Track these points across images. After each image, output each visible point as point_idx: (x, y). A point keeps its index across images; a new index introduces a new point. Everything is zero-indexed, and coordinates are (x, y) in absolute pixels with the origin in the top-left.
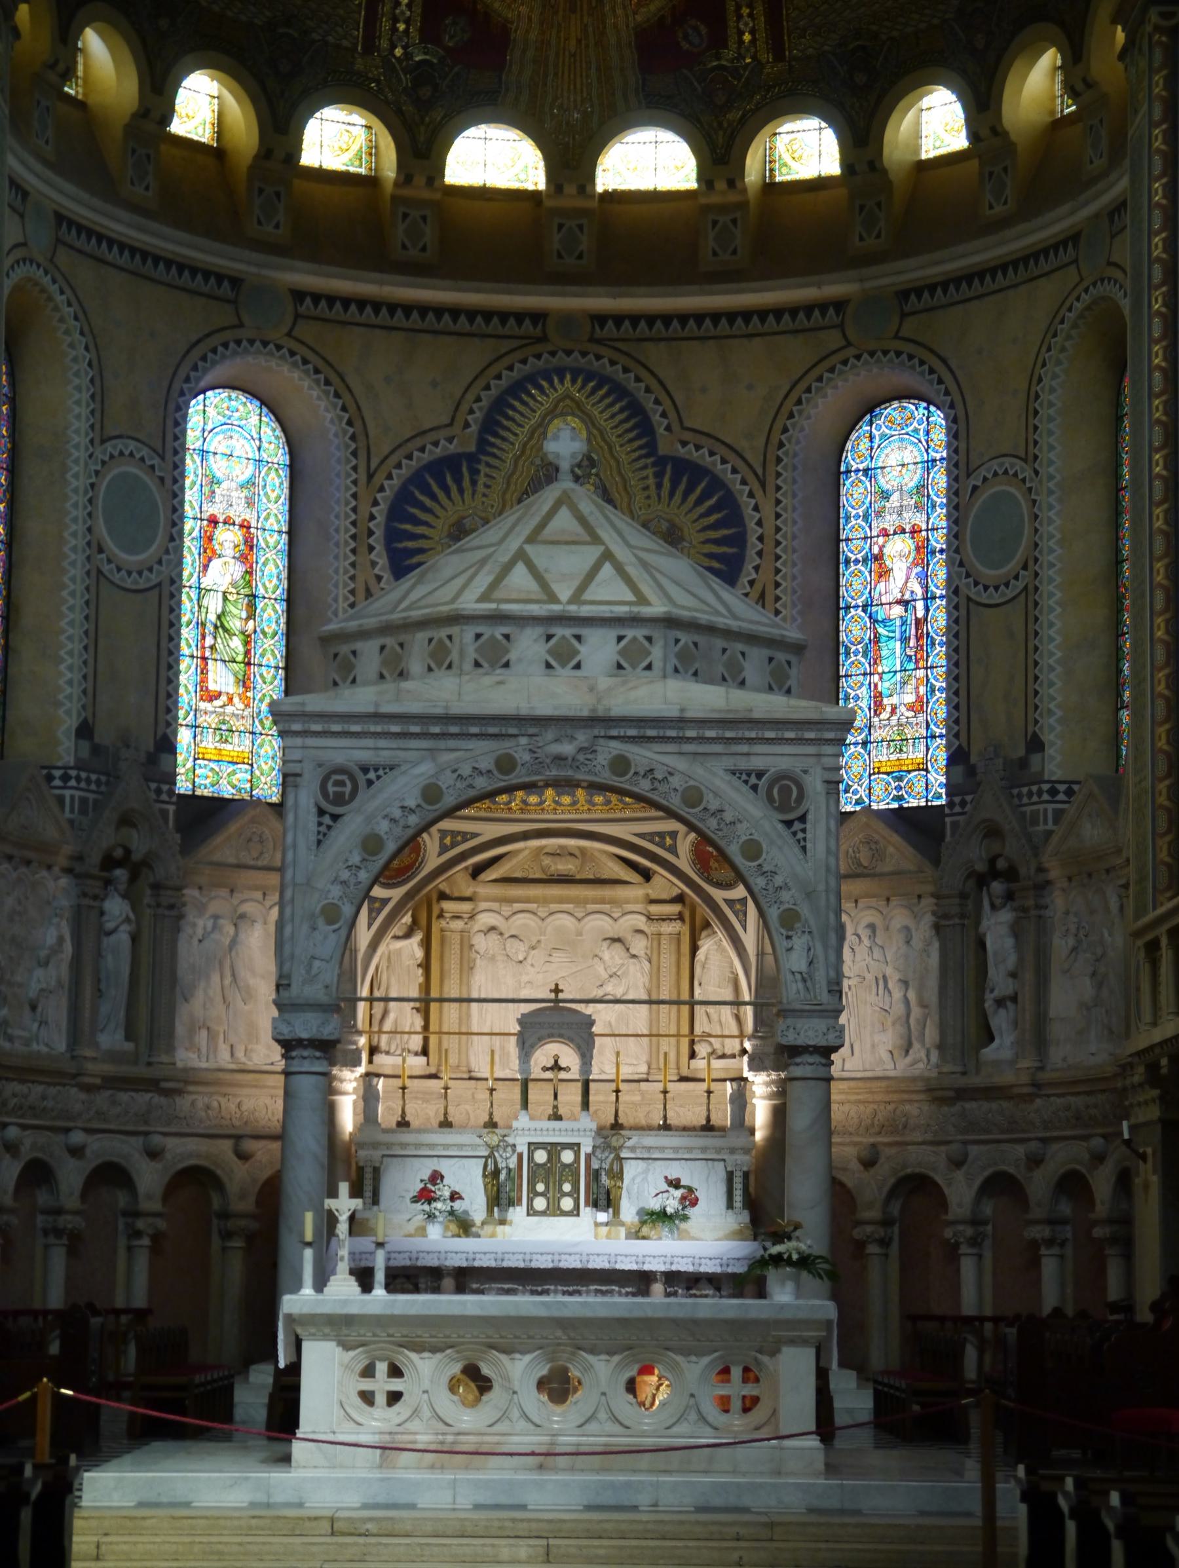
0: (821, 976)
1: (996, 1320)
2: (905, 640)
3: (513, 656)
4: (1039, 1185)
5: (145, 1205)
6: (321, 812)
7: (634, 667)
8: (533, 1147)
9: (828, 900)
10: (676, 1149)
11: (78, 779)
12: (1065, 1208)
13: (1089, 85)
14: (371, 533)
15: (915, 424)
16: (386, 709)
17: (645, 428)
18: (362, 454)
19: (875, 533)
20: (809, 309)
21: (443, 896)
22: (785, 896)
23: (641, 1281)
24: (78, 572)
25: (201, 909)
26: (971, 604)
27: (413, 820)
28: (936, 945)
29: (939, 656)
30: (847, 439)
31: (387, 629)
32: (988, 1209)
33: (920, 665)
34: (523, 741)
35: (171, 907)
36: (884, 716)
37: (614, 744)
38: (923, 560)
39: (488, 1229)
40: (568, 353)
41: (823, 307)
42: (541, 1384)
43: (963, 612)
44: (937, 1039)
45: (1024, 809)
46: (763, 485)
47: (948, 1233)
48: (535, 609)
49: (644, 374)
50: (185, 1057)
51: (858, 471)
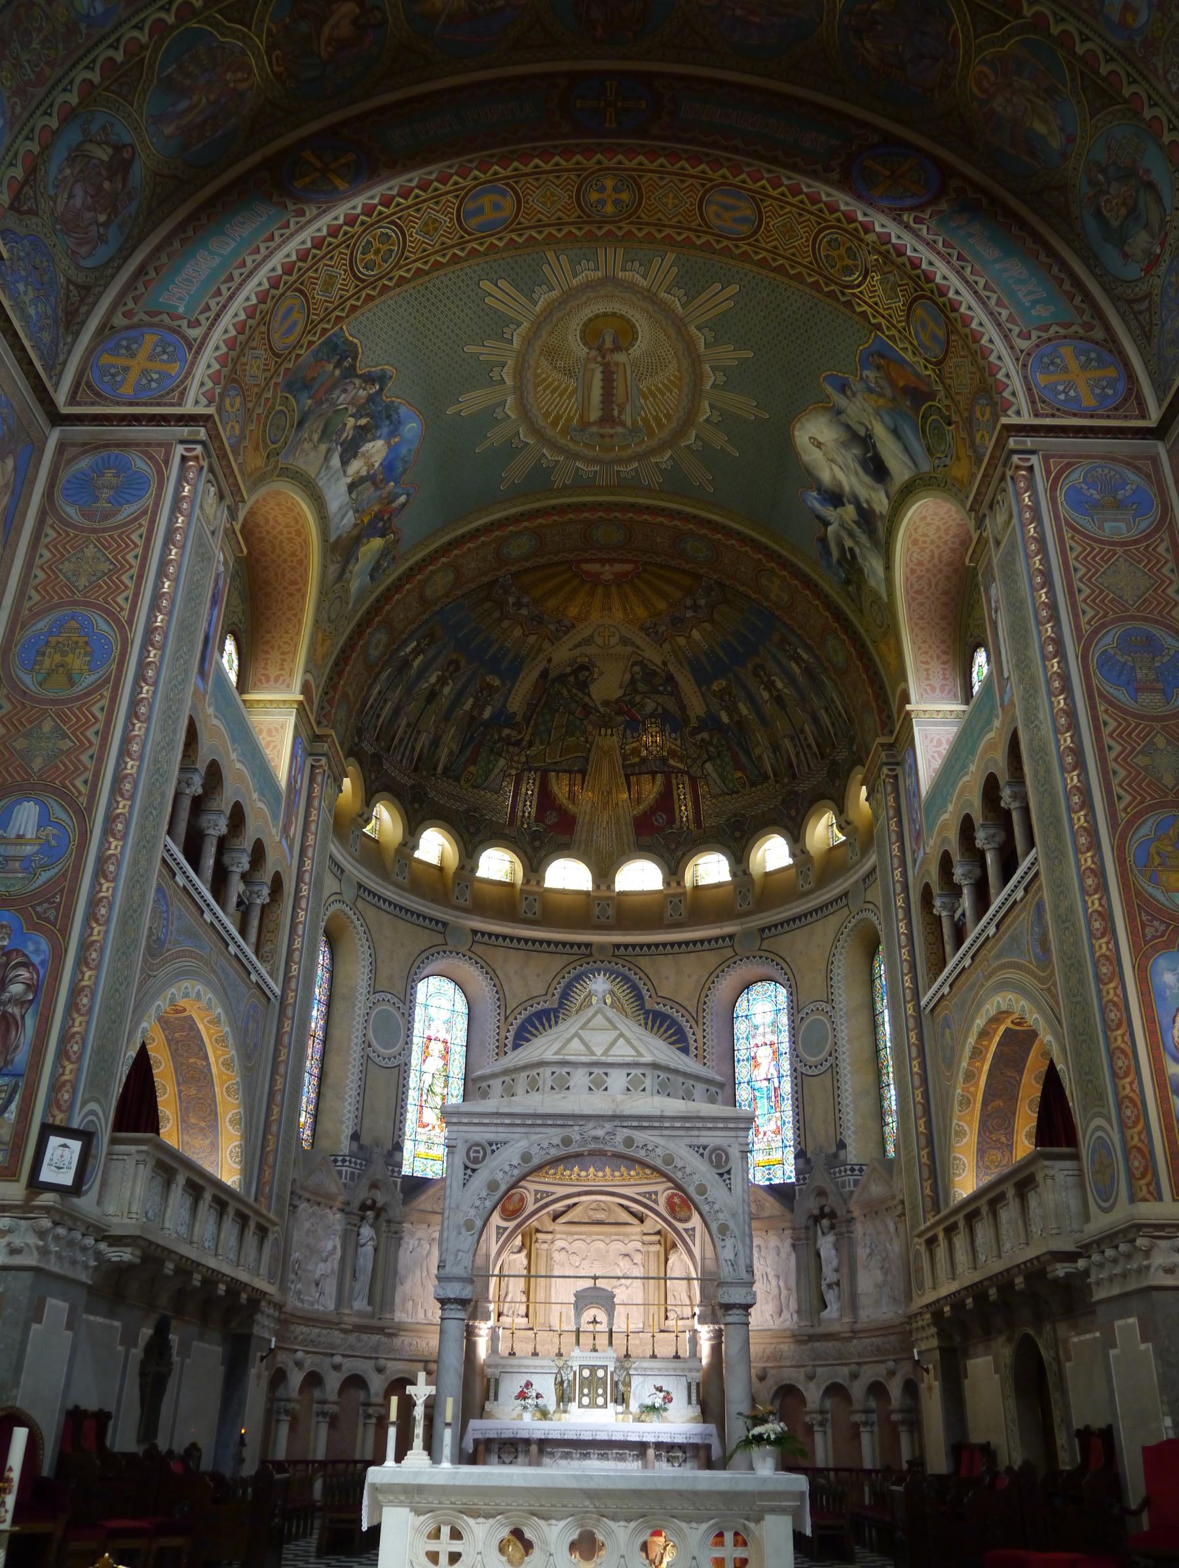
0: (742, 1262)
1: (836, 1470)
2: (769, 1098)
3: (571, 1084)
4: (857, 1390)
5: (374, 1400)
6: (466, 1168)
7: (636, 1090)
8: (582, 1367)
10: (660, 1370)
11: (350, 1162)
12: (873, 1404)
13: (848, 823)
14: (506, 1045)
16: (502, 1110)
17: (639, 997)
18: (503, 1007)
20: (717, 939)
21: (538, 1231)
22: (720, 1215)
23: (640, 1448)
24: (357, 1056)
25: (412, 1234)
27: (516, 1172)
28: (793, 1256)
29: (787, 1105)
31: (506, 1072)
32: (828, 1404)
34: (576, 1128)
35: (396, 1233)
36: (761, 1136)
37: (625, 1130)
39: (557, 1415)
40: (602, 962)
41: (723, 938)
42: (573, 1546)
43: (799, 1080)
44: (796, 1308)
46: (697, 1023)
47: (807, 1419)
48: (584, 1059)
49: (638, 971)
50: (400, 1316)
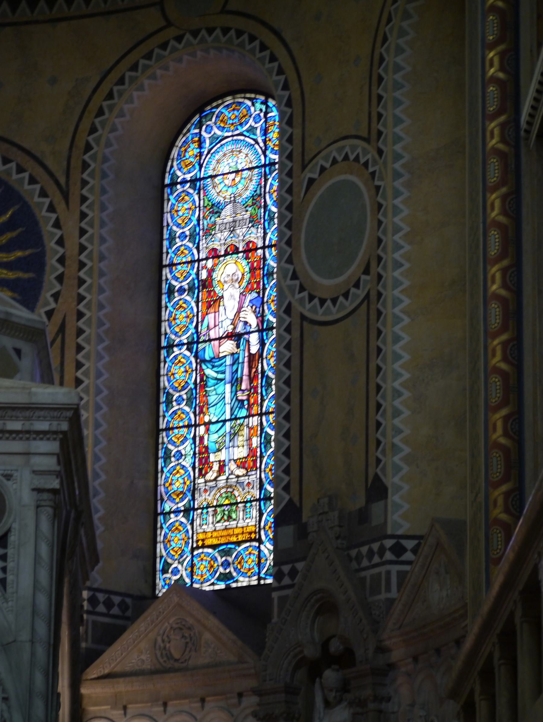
2: (236, 382)
9: (33, 654)
15: (251, 122)
19: (203, 255)
26: (305, 323)
30: (172, 145)
33: (253, 412)
36: (211, 475)
38: (258, 283)
43: (296, 333)
45: (363, 574)
46: (66, 196)
51: (184, 182)
